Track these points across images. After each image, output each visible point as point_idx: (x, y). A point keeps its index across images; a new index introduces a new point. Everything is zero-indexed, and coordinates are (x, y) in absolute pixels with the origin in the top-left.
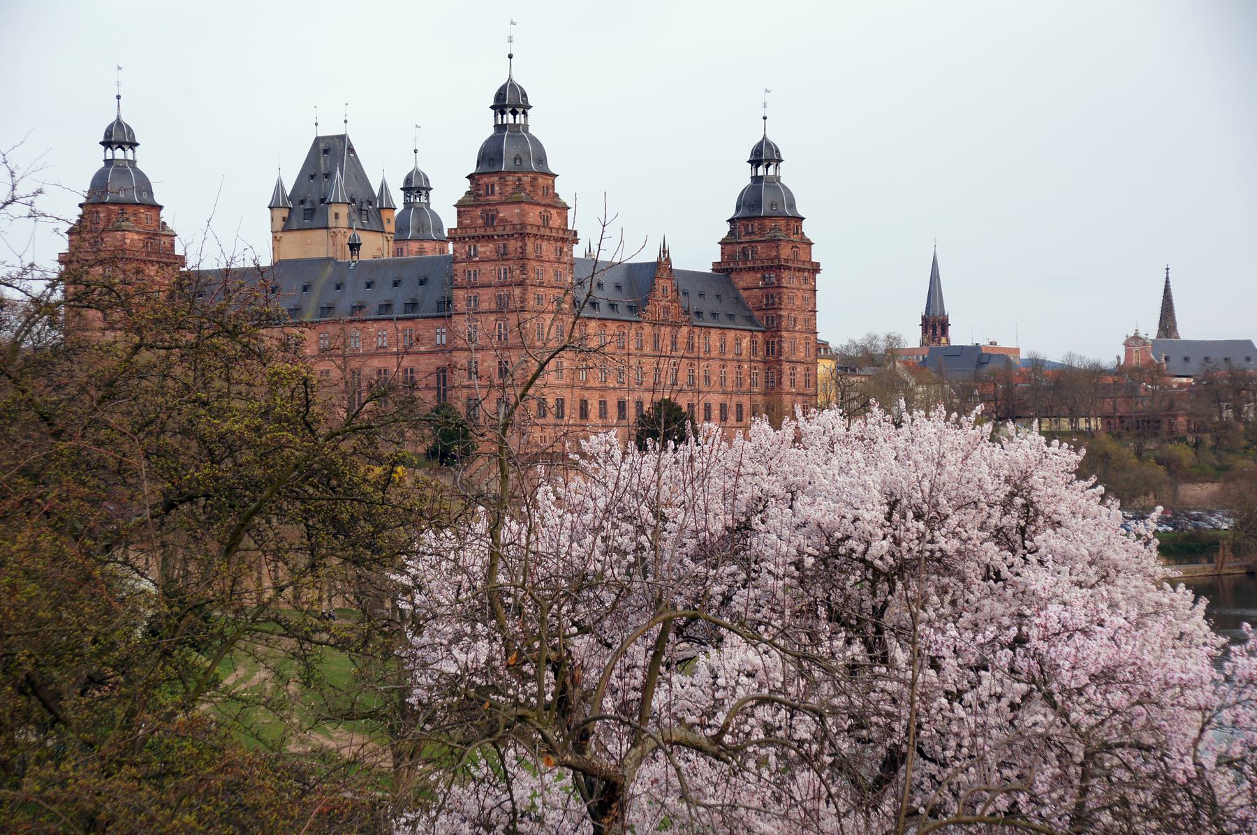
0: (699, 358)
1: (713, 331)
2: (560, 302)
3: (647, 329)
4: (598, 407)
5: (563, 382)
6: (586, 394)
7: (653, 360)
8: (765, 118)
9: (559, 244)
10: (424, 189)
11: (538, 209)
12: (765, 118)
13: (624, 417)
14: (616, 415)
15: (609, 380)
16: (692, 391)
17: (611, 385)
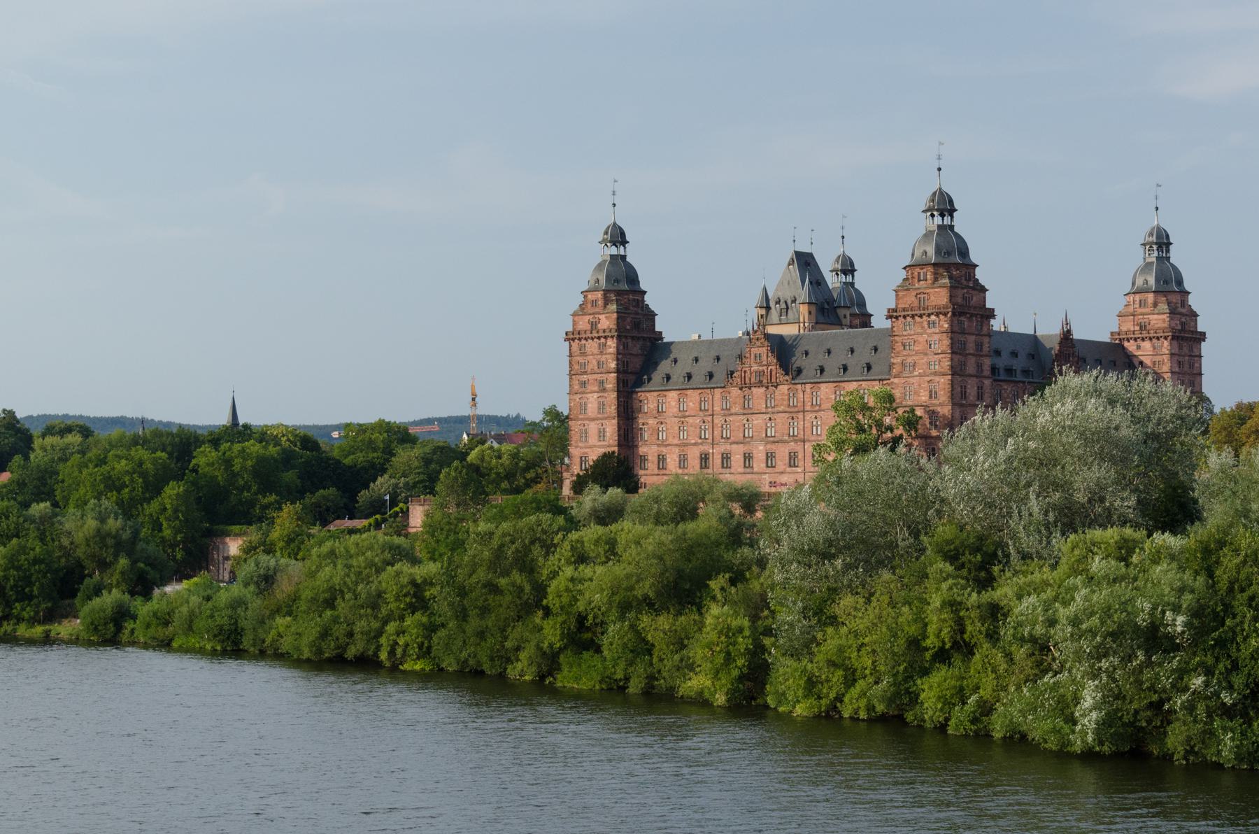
0: (804, 411)
1: (823, 386)
2: (601, 383)
3: (735, 391)
4: (677, 460)
5: (606, 443)
6: (664, 450)
7: (742, 417)
8: (939, 169)
9: (603, 340)
10: (1164, 244)
11: (588, 317)
12: (939, 169)
13: (706, 467)
14: (699, 466)
15: (689, 438)
16: (796, 441)
17: (693, 442)
